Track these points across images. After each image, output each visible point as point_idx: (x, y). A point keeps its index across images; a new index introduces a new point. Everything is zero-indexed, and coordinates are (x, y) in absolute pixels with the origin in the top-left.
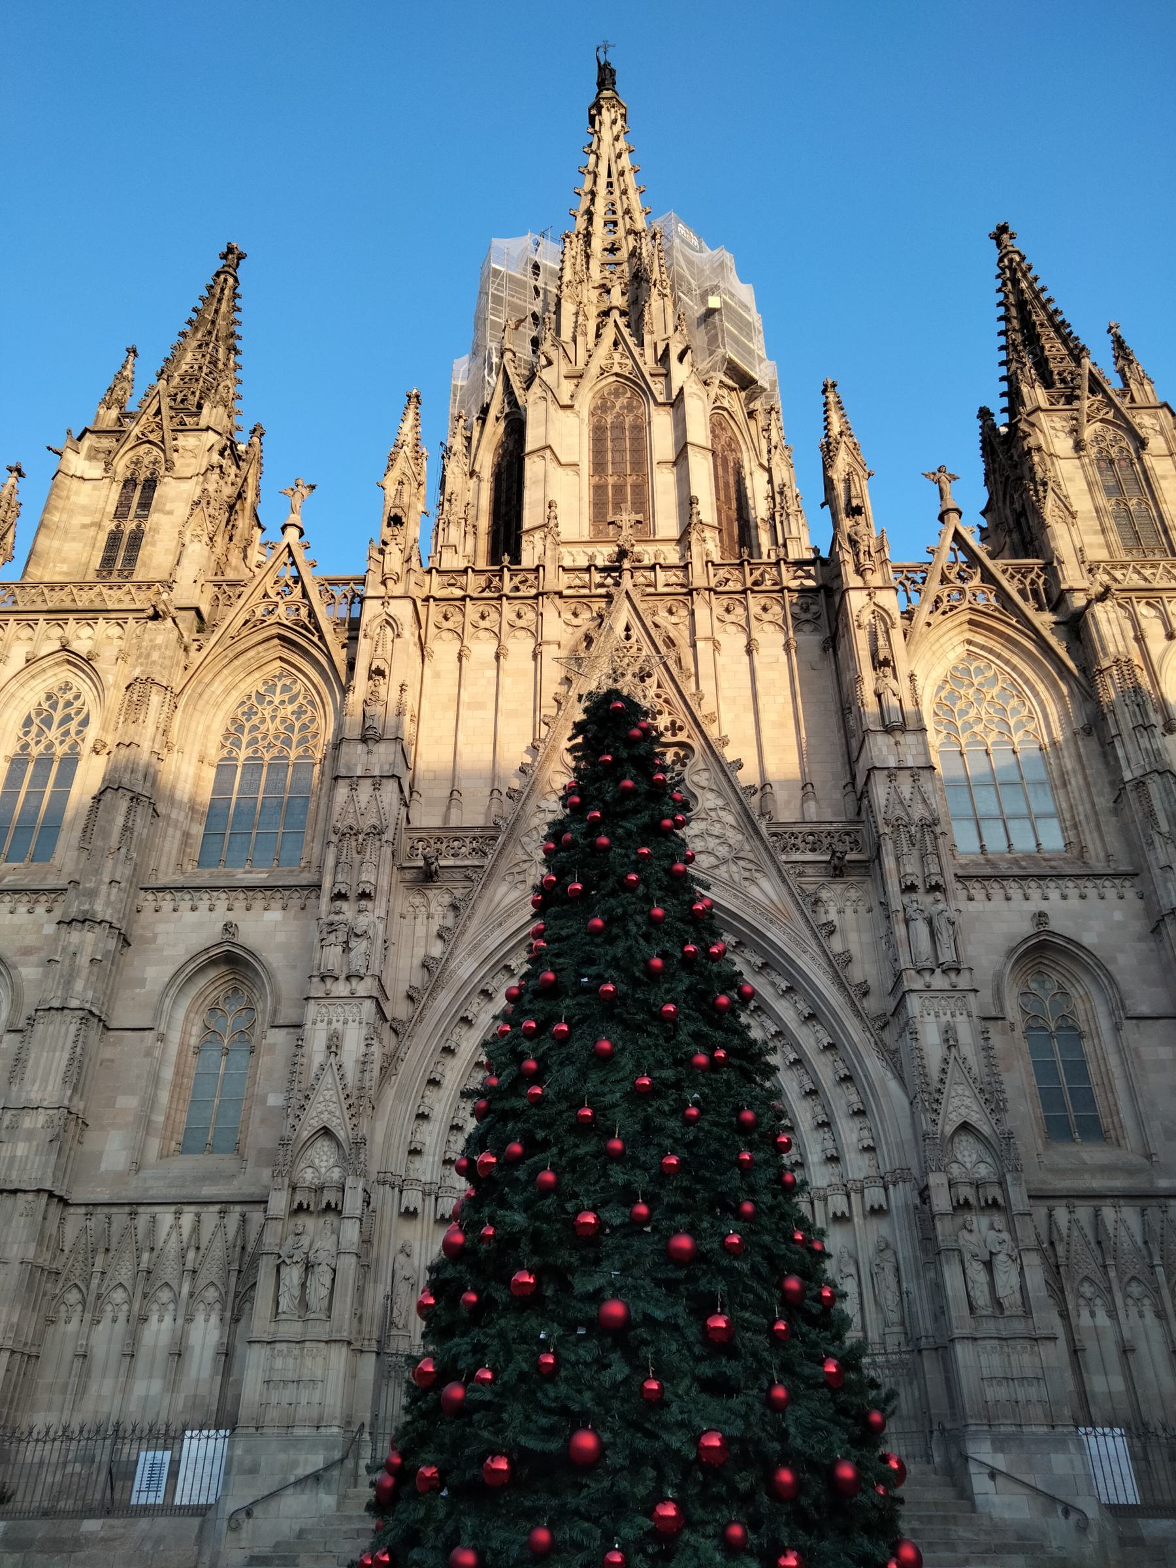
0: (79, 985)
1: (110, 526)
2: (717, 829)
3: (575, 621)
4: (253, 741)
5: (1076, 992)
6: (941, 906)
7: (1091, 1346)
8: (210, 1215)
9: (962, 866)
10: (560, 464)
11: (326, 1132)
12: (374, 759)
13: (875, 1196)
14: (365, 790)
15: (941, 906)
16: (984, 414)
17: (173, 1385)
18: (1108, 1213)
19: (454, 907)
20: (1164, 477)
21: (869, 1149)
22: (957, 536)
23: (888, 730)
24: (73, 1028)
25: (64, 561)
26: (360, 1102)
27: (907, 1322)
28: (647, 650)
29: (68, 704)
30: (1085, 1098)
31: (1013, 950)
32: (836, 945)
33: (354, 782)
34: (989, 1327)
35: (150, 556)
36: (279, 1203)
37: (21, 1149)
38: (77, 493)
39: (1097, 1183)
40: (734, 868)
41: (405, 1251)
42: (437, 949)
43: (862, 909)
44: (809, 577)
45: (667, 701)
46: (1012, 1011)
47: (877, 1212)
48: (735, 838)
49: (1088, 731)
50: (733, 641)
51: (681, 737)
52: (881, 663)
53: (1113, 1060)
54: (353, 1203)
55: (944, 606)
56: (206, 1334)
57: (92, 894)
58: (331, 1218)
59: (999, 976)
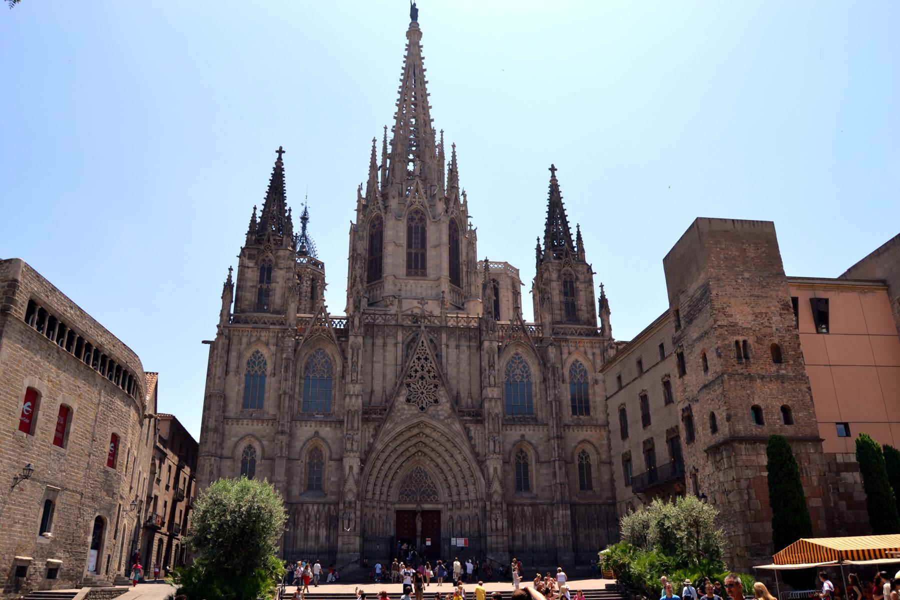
1: (259, 286)
4: (314, 371)
5: (529, 454)
9: (506, 420)
11: (350, 490)
13: (475, 503)
16: (538, 239)
18: (526, 508)
26: (357, 482)
27: (479, 531)
28: (428, 351)
29: (259, 358)
30: (527, 480)
31: (514, 445)
32: (473, 442)
33: (351, 396)
42: (371, 441)
46: (513, 460)
48: (450, 411)
50: (453, 343)
52: (492, 366)
54: (358, 507)
56: (323, 533)
57: (283, 425)
59: (510, 451)
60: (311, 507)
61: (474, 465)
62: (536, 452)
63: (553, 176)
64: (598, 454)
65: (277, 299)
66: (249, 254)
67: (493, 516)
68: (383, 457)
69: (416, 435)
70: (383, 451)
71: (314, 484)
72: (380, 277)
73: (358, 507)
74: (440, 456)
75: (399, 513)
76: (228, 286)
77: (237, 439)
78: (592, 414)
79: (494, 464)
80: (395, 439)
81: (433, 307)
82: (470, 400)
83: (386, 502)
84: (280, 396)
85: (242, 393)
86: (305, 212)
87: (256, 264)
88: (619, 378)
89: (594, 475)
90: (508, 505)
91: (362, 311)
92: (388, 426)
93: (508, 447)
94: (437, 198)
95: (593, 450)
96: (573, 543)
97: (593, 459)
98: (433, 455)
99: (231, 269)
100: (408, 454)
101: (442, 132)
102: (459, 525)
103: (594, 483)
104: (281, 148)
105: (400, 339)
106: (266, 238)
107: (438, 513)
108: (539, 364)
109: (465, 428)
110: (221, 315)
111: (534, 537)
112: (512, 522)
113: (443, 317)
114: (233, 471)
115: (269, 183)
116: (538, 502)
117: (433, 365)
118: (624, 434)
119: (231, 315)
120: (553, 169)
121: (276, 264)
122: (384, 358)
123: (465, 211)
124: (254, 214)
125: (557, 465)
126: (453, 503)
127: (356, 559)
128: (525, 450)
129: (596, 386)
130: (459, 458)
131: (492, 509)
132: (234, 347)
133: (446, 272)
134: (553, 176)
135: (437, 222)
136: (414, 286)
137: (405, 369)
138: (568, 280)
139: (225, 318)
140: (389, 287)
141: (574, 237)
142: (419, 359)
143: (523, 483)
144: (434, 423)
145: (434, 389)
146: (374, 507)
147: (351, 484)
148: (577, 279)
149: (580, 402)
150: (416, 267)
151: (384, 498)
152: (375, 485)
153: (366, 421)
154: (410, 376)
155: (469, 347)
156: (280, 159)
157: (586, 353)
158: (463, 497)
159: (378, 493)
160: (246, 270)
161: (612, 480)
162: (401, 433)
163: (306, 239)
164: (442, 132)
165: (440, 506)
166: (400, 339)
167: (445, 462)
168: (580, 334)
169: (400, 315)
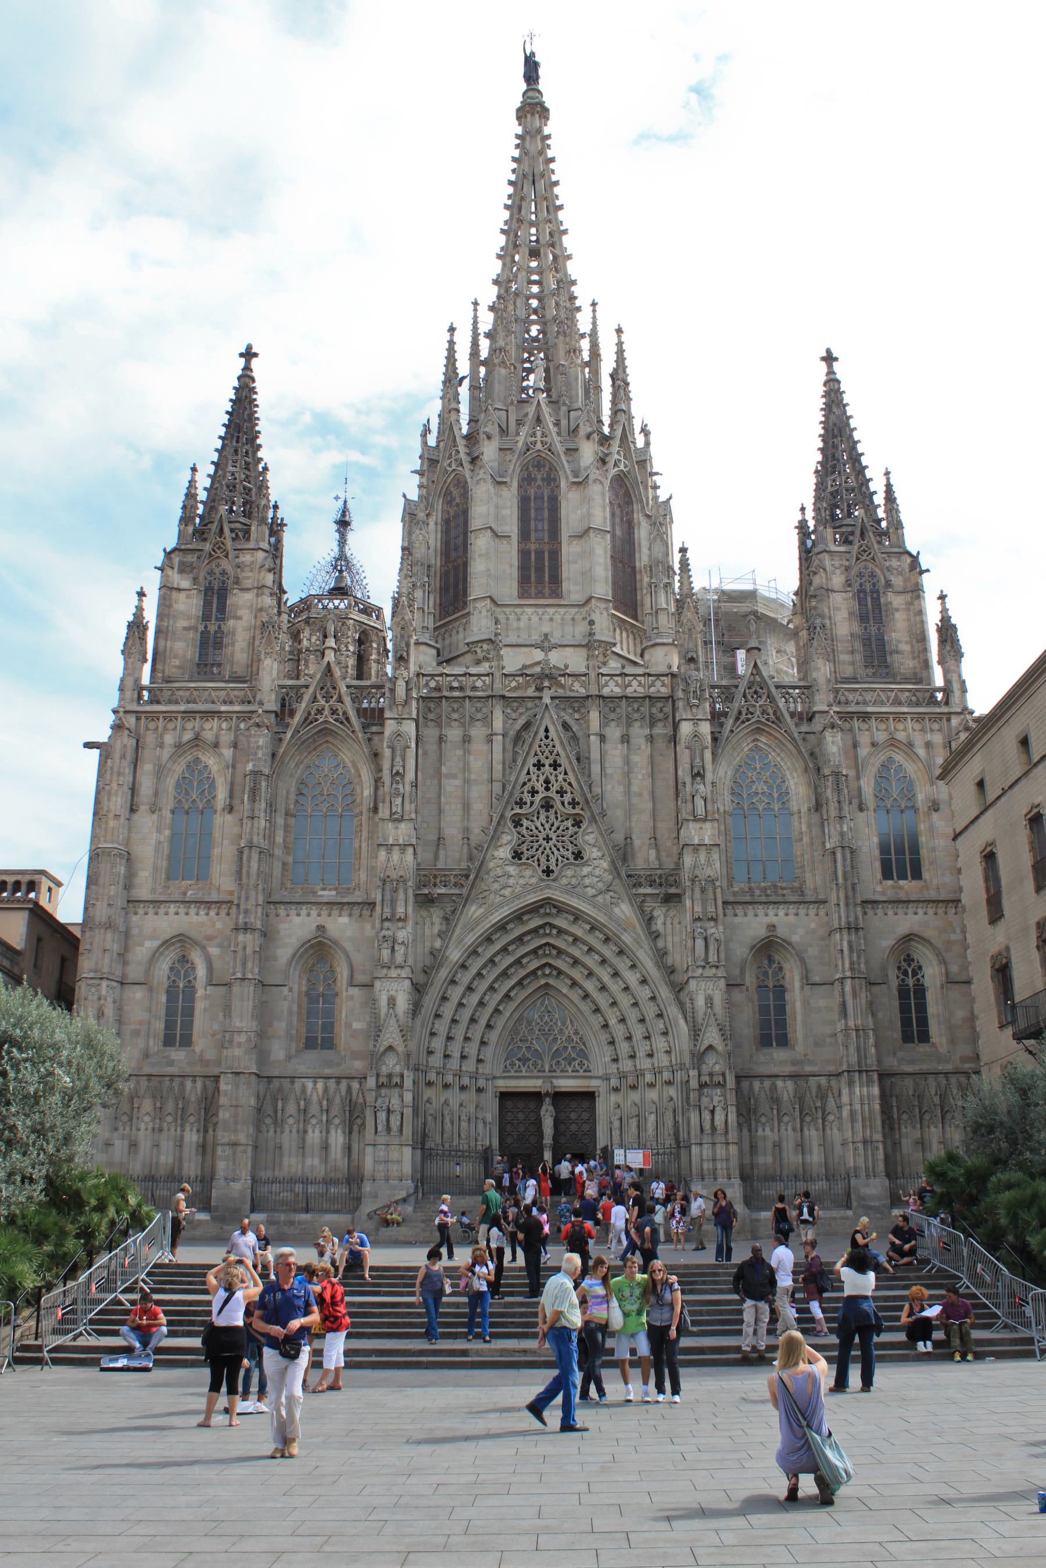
0: (250, 965)
1: (201, 628)
2: (597, 872)
3: (514, 716)
5: (786, 967)
6: (713, 930)
7: (760, 1144)
8: (332, 1083)
9: (735, 894)
10: (497, 536)
12: (400, 832)
13: (666, 1076)
14: (396, 855)
15: (713, 930)
16: (803, 509)
17: (325, 1159)
18: (779, 1083)
19: (446, 919)
20: (897, 610)
21: (668, 1052)
22: (755, 665)
23: (696, 819)
24: (252, 989)
25: (176, 657)
26: (405, 1033)
28: (559, 748)
33: (389, 848)
34: (706, 1139)
35: (233, 654)
36: (371, 1082)
37: (237, 1052)
38: (177, 601)
39: (775, 1070)
40: (607, 897)
41: (428, 1101)
42: (438, 944)
43: (676, 922)
44: (663, 685)
45: (570, 784)
46: (750, 980)
47: (669, 1083)
49: (817, 810)
50: (614, 732)
51: (577, 811)
52: (698, 775)
53: (798, 1005)
54: (408, 1083)
55: (743, 717)
56: (337, 1139)
57: (246, 912)
58: (397, 1090)
59: (744, 962)
60: (310, 1085)
61: (665, 993)
62: (802, 961)
63: (831, 372)
64: (943, 962)
65: (238, 650)
66: (182, 563)
67: (705, 1100)
68: (465, 978)
69: (535, 931)
70: (464, 967)
71: (319, 1037)
72: (465, 603)
73: (408, 1083)
74: (591, 974)
75: (505, 1097)
76: (137, 627)
77: (156, 944)
78: (926, 875)
79: (706, 992)
80: (489, 940)
81: (575, 660)
82: (653, 853)
83: (474, 1077)
84: (241, 852)
85: (166, 849)
86: (344, 511)
87: (195, 580)
88: (981, 784)
89: (933, 1009)
90: (738, 1078)
91: (413, 668)
92: (474, 911)
93: (741, 951)
94: (583, 431)
95: (930, 955)
96: (887, 1158)
97: (932, 974)
98: (576, 974)
99: (141, 594)
100: (522, 973)
101: (594, 304)
102: (635, 1120)
103: (934, 1028)
104: (249, 347)
105: (498, 724)
106: (214, 527)
107: (589, 1096)
108: (806, 770)
109: (642, 912)
110: (121, 689)
111: (802, 1147)
112: (747, 1113)
113: (593, 675)
114: (149, 1010)
115: (225, 419)
116: (808, 1069)
117: (571, 778)
118: (995, 911)
119: (143, 688)
120: (829, 358)
121: (237, 581)
122: (466, 768)
123: (643, 461)
124: (192, 483)
125: (848, 988)
126: (622, 1076)
127: (403, 1194)
128: (777, 957)
129: (935, 816)
130: (632, 978)
131: (702, 1086)
132: (146, 754)
133: (603, 588)
134: (831, 372)
135: (581, 484)
136: (535, 619)
137: (509, 788)
138: (868, 587)
139: (128, 694)
140: (480, 624)
141: (879, 499)
142: (539, 765)
143: (773, 1030)
144: (574, 902)
145: (572, 830)
146: (446, 1086)
147: (391, 1036)
148: (888, 584)
149: (900, 851)
150: (540, 580)
151: (470, 1066)
152: (449, 1038)
153: (426, 901)
154: (521, 803)
155: (651, 739)
156: (247, 368)
157: (910, 745)
158: (645, 1063)
159: (457, 1055)
160: (174, 594)
161: (972, 1018)
162: (502, 927)
163: (346, 560)
164: (594, 304)
165: (593, 1084)
166: (498, 724)
167: (603, 988)
168: (897, 702)
169: (497, 675)
